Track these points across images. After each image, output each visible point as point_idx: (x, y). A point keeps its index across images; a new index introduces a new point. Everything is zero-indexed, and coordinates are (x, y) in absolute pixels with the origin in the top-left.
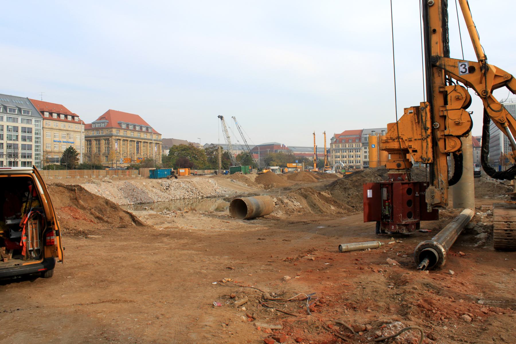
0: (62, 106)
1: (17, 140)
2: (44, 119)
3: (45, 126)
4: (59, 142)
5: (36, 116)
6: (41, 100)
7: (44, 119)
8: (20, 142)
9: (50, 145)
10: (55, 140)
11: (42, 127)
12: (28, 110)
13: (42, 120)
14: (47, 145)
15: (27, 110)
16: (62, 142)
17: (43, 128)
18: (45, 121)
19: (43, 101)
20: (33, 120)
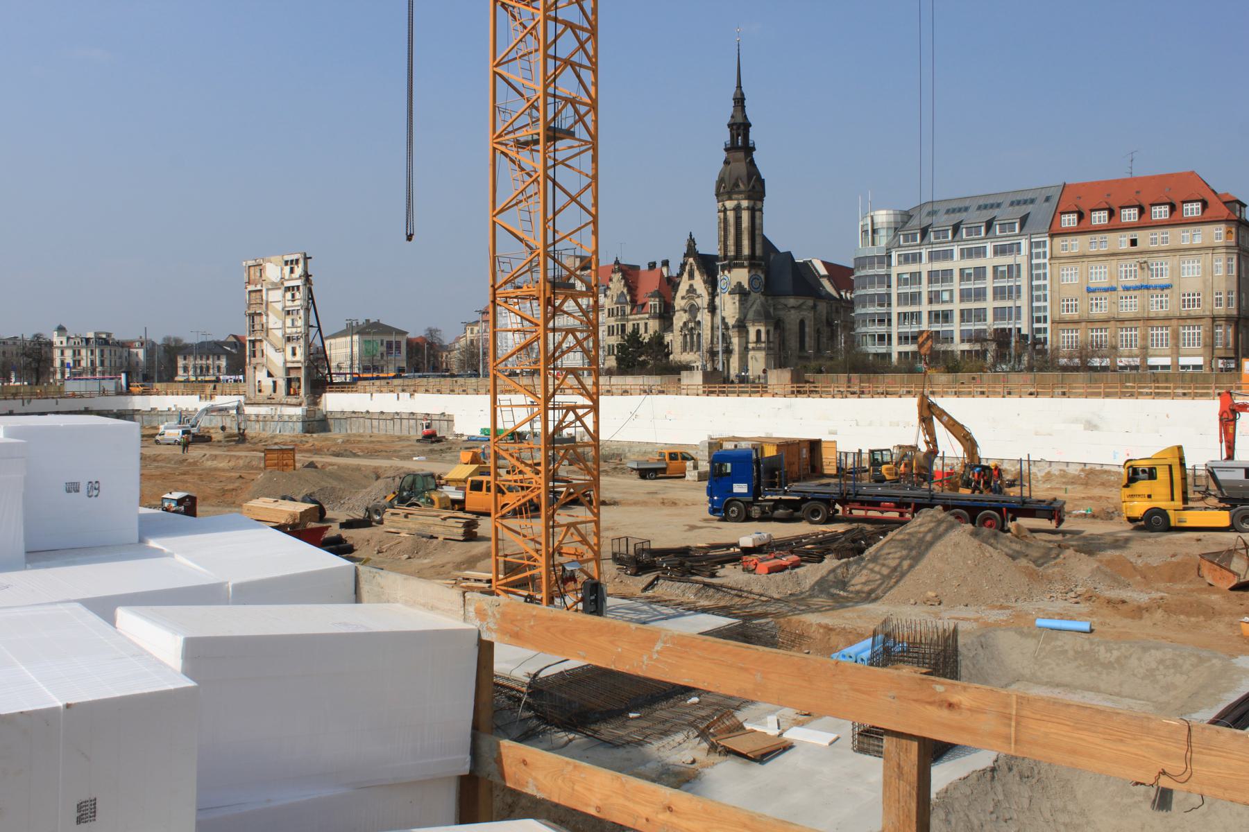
0: (1192, 177)
1: (951, 301)
2: (1052, 236)
3: (1056, 253)
4: (1106, 290)
5: (1040, 231)
6: (1125, 175)
7: (1052, 236)
8: (990, 304)
9: (1074, 303)
10: (1128, 284)
11: (1048, 256)
12: (1010, 221)
13: (1048, 239)
14: (1065, 303)
15: (1006, 222)
16: (1120, 289)
17: (1052, 258)
18: (1057, 240)
19: (1135, 175)
20: (1024, 244)
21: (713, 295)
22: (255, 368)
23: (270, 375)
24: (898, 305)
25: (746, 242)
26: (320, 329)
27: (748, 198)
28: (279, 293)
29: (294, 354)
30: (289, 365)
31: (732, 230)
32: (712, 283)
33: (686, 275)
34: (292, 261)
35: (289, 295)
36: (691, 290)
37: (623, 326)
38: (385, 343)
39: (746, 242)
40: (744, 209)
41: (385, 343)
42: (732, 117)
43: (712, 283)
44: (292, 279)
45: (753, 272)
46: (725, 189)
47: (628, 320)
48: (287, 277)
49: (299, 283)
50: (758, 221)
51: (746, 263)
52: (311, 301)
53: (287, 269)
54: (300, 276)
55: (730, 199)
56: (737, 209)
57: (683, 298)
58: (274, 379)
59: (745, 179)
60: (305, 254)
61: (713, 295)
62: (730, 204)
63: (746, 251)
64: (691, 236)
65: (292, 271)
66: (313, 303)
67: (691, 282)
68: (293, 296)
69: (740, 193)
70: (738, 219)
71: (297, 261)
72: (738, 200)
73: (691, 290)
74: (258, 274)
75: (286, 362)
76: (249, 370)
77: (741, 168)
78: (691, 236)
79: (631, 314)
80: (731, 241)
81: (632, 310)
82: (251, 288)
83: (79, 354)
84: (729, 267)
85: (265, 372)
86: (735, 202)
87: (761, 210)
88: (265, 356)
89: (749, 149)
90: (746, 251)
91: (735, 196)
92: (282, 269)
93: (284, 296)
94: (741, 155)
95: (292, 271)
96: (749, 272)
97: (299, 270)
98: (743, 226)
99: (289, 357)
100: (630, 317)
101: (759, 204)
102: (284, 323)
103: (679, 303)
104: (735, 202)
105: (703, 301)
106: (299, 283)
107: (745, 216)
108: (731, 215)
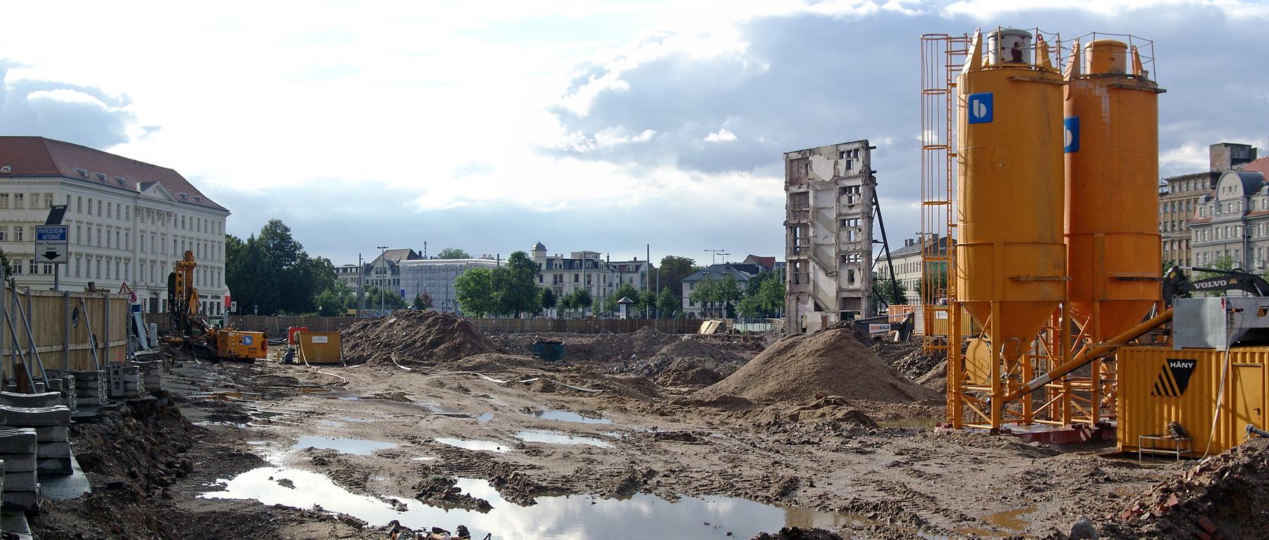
22: (798, 299)
23: (818, 308)
26: (886, 246)
28: (833, 195)
29: (852, 280)
30: (846, 295)
34: (849, 152)
35: (845, 199)
44: (850, 178)
48: (842, 175)
49: (859, 182)
52: (874, 207)
53: (843, 163)
54: (860, 172)
58: (824, 314)
60: (866, 142)
65: (849, 167)
66: (878, 209)
68: (850, 200)
71: (856, 151)
74: (803, 171)
75: (840, 290)
76: (790, 302)
82: (794, 189)
83: (561, 280)
85: (810, 304)
88: (811, 283)
92: (836, 164)
93: (838, 200)
95: (849, 167)
97: (857, 166)
99: (845, 284)
102: (838, 237)
106: (859, 182)
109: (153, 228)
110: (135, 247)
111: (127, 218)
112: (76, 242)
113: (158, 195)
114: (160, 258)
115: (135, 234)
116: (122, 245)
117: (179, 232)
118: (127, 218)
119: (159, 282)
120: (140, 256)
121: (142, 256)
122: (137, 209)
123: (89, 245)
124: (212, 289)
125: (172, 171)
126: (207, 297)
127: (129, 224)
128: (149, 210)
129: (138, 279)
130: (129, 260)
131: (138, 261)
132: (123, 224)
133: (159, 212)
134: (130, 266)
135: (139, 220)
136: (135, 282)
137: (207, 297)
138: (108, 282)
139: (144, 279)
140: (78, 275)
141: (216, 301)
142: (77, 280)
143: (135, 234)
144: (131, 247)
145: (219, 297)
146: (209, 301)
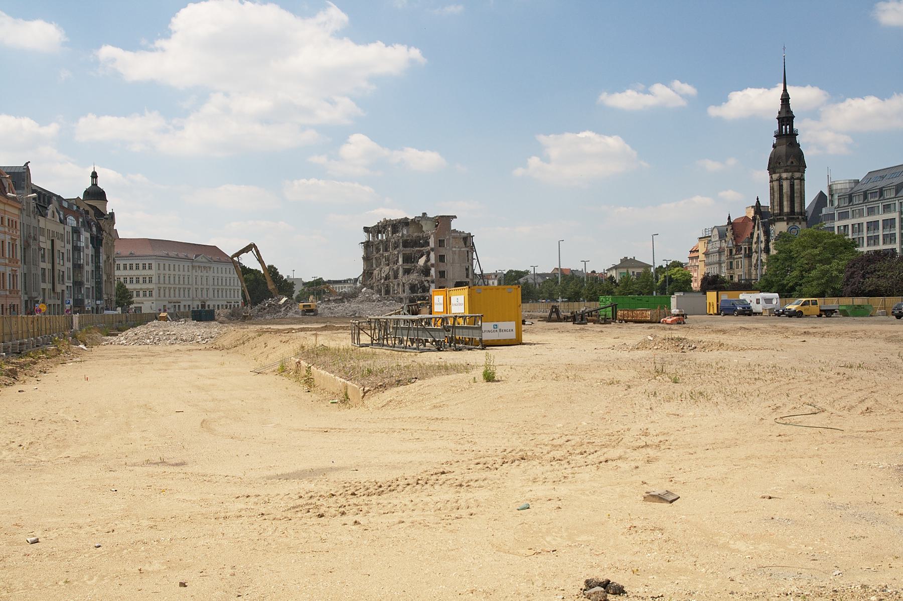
21: (767, 241)
24: (868, 245)
25: (786, 203)
27: (786, 171)
31: (777, 195)
32: (767, 233)
33: (756, 227)
36: (758, 238)
37: (731, 263)
38: (635, 274)
39: (786, 203)
40: (784, 180)
41: (635, 274)
42: (779, 113)
43: (767, 233)
45: (791, 224)
46: (773, 166)
47: (734, 259)
50: (796, 187)
51: (785, 218)
55: (775, 173)
56: (780, 179)
57: (755, 243)
59: (784, 158)
61: (767, 241)
62: (775, 176)
63: (786, 209)
64: (758, 199)
67: (759, 232)
69: (781, 168)
70: (781, 186)
72: (780, 173)
73: (758, 238)
77: (783, 149)
78: (758, 199)
79: (736, 254)
80: (776, 204)
81: (736, 251)
84: (773, 222)
86: (778, 175)
87: (802, 180)
89: (793, 134)
90: (786, 209)
91: (777, 170)
94: (784, 141)
96: (788, 224)
98: (784, 191)
100: (736, 257)
101: (797, 175)
103: (754, 246)
104: (778, 175)
105: (763, 246)
107: (786, 185)
108: (776, 184)
109: (202, 274)
110: (192, 281)
111: (188, 271)
112: (163, 283)
113: (204, 260)
114: (205, 287)
115: (192, 277)
116: (186, 282)
117: (216, 274)
118: (188, 271)
119: (200, 297)
120: (195, 286)
121: (197, 287)
122: (193, 267)
123: (174, 284)
124: (234, 299)
125: (215, 248)
126: (231, 302)
127: (190, 273)
128: (199, 267)
129: (195, 296)
130: (190, 288)
131: (194, 289)
132: (186, 273)
133: (205, 267)
134: (191, 291)
135: (194, 271)
136: (193, 298)
137: (231, 302)
138: (179, 298)
139: (198, 296)
140: (164, 296)
141: (236, 304)
142: (164, 298)
143: (192, 277)
144: (190, 283)
145: (238, 302)
146: (233, 304)
